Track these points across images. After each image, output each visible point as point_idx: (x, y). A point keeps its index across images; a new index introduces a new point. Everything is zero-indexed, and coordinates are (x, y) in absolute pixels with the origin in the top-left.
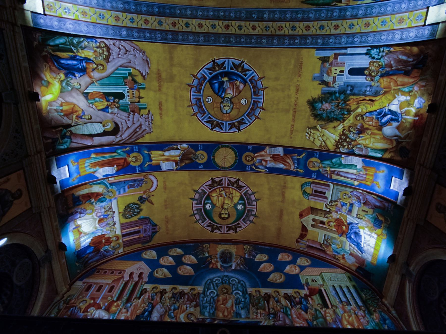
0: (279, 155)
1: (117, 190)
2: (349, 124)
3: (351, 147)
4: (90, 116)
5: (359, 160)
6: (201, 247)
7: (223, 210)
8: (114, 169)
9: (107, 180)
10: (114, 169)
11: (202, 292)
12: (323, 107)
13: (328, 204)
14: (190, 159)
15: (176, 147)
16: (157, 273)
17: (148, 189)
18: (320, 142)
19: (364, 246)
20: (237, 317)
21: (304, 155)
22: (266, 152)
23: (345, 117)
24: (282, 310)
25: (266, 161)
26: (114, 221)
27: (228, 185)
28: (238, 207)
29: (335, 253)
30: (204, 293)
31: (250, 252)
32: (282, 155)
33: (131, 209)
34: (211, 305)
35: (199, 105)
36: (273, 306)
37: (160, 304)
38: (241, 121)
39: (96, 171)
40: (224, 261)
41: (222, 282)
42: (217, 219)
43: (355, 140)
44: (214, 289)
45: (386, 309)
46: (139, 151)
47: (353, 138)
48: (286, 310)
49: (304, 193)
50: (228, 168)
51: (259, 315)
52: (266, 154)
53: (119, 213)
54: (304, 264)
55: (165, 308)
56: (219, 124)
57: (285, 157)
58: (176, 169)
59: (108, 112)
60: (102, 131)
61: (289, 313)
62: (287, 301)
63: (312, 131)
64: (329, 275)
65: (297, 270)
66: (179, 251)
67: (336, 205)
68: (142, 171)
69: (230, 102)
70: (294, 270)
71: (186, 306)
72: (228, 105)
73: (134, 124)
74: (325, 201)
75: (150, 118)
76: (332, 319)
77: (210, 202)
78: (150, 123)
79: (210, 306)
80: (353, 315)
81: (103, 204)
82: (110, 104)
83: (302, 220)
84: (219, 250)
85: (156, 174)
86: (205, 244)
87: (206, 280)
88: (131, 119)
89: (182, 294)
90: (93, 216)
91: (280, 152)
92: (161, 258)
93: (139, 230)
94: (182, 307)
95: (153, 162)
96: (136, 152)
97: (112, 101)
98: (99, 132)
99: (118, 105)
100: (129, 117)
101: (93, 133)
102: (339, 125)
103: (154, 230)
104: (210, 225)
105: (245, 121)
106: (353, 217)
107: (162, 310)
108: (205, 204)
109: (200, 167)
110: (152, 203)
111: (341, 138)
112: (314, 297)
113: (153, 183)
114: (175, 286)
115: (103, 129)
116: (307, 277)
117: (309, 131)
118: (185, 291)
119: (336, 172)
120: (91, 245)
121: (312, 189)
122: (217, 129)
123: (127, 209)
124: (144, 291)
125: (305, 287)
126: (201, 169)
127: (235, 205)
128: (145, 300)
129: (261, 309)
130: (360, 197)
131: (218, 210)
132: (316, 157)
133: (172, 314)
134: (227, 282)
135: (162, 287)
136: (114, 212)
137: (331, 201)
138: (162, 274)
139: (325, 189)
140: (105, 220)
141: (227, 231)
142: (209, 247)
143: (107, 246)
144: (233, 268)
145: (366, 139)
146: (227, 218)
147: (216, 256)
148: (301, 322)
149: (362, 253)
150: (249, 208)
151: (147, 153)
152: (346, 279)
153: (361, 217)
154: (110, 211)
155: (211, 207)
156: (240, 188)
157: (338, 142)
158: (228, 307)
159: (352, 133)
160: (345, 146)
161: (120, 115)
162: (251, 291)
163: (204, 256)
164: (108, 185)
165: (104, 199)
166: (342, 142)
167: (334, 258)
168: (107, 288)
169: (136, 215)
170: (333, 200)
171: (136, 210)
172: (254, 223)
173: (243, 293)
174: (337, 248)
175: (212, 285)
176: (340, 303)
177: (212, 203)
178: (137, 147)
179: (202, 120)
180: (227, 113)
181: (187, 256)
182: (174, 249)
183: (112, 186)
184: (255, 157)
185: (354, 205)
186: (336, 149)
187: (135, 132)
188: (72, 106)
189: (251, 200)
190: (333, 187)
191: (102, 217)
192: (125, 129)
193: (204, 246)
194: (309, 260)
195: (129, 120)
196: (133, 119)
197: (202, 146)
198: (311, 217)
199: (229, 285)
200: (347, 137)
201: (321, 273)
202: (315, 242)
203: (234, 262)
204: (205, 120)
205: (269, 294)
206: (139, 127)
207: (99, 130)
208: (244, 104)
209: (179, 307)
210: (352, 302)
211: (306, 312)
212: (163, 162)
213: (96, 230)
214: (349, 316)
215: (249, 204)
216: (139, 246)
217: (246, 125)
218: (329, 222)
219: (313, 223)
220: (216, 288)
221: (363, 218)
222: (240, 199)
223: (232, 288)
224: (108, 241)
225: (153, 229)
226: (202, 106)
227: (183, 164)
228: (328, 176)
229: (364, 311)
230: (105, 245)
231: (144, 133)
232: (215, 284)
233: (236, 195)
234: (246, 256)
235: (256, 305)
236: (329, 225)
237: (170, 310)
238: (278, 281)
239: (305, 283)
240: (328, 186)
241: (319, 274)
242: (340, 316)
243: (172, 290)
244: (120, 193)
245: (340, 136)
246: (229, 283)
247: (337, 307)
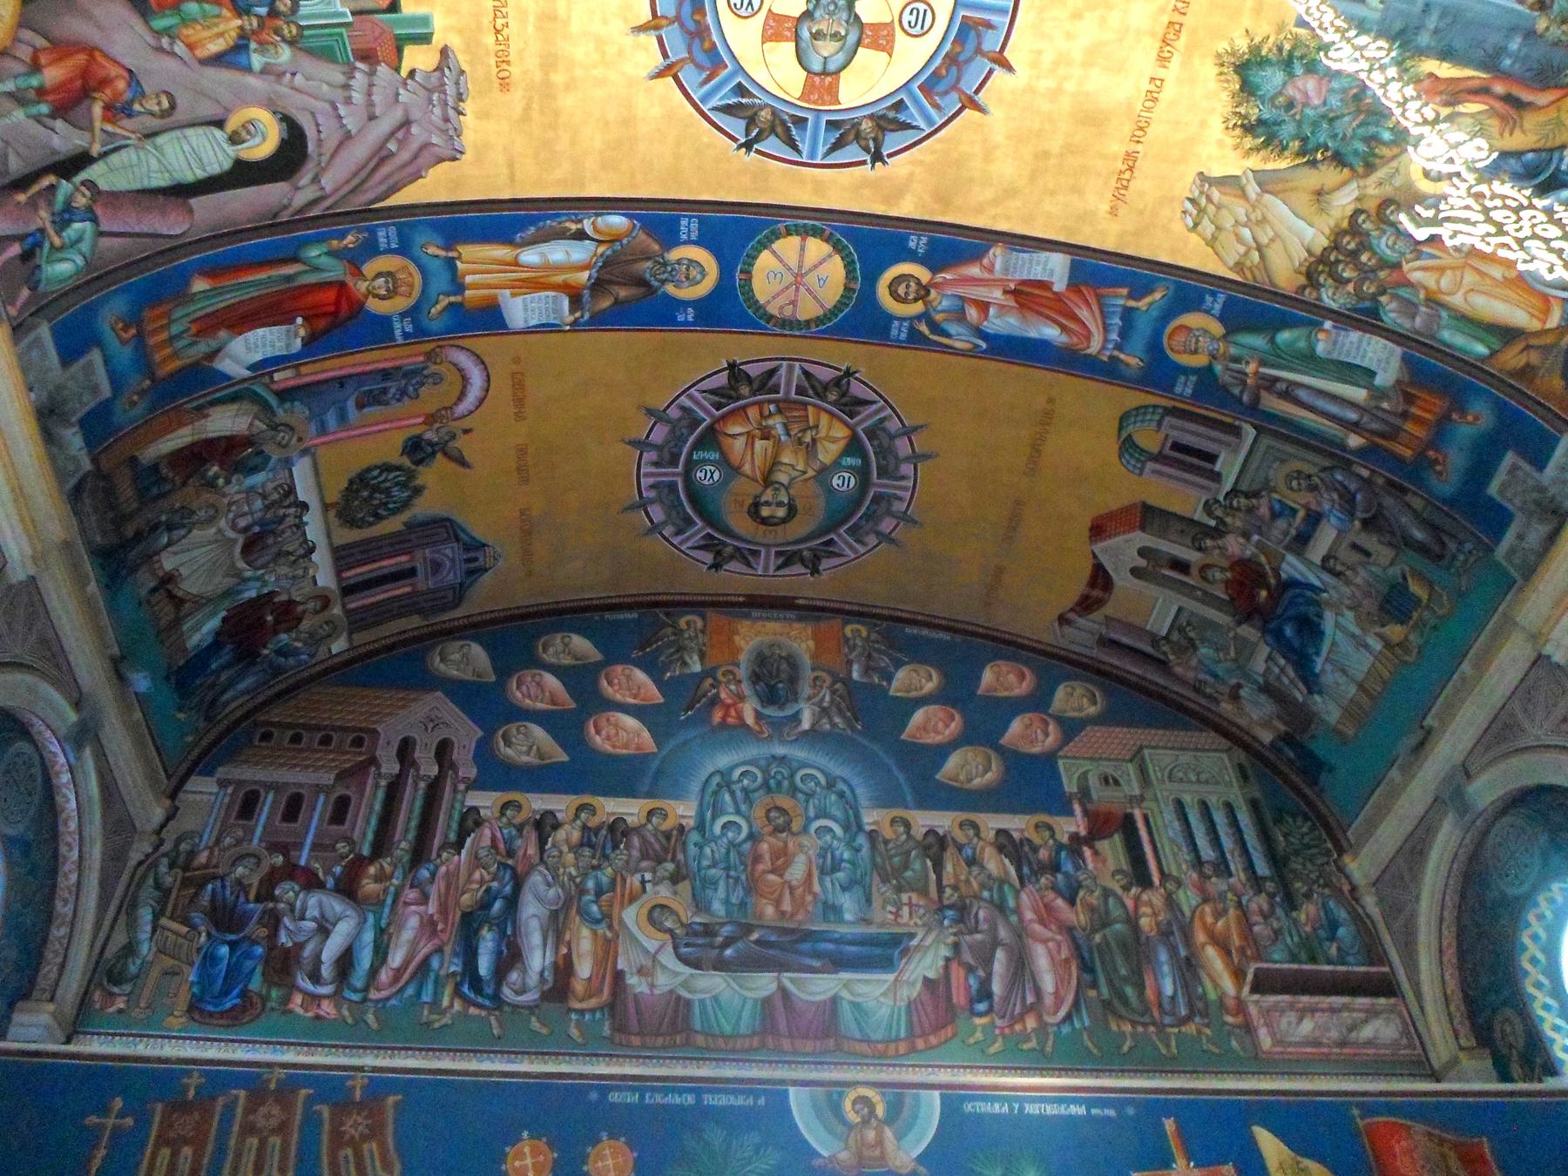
0: (1044, 285)
1: (310, 419)
2: (1387, 190)
3: (1372, 290)
4: (168, 94)
5: (1391, 353)
6: (669, 630)
7: (769, 492)
8: (296, 335)
9: (266, 380)
10: (296, 335)
11: (692, 823)
12: (1290, 91)
13: (1217, 501)
14: (641, 282)
15: (574, 227)
16: (508, 743)
17: (446, 408)
18: (1242, 249)
19: (1323, 670)
20: (826, 920)
21: (1158, 295)
22: (991, 270)
23: (1375, 155)
24: (986, 894)
25: (983, 306)
26: (306, 541)
27: (801, 391)
28: (836, 481)
29: (1202, 676)
30: (701, 826)
31: (869, 656)
32: (1060, 285)
33: (376, 489)
34: (732, 873)
35: (691, 26)
36: (956, 876)
37: (541, 868)
38: (891, 114)
39: (218, 351)
40: (770, 697)
41: (766, 785)
42: (740, 523)
43: (1397, 266)
44: (738, 812)
45: (1346, 888)
46: (404, 250)
47: (1388, 252)
48: (1003, 898)
49: (1128, 446)
50: (808, 322)
51: (906, 910)
52: (986, 275)
53: (326, 507)
54: (1081, 709)
55: (563, 886)
56: (783, 123)
57: (1072, 296)
58: (575, 323)
59: (248, 69)
60: (227, 165)
61: (1011, 903)
62: (1007, 861)
63: (1216, 194)
64: (1166, 758)
65: (1049, 739)
66: (580, 643)
67: (1250, 510)
68: (420, 333)
69: (844, 16)
70: (1040, 736)
71: (638, 877)
72: (835, 28)
73: (372, 117)
74: (1208, 489)
75: (450, 89)
76: (1158, 924)
77: (714, 456)
78: (451, 113)
79: (728, 876)
80: (1232, 912)
81: (258, 479)
82: (255, 22)
83: (1098, 548)
84: (742, 643)
85: (484, 344)
86: (688, 613)
87: (704, 775)
88: (357, 97)
89: (618, 830)
90: (220, 531)
91: (1052, 272)
92: (510, 675)
93: (408, 566)
94: (624, 880)
95: (468, 293)
96: (389, 251)
97: (263, 11)
98: (214, 169)
99: (294, 31)
100: (346, 87)
101: (189, 177)
102: (1344, 184)
103: (472, 565)
104: (708, 544)
105: (912, 116)
106: (1309, 563)
107: (552, 892)
108: (691, 466)
109: (680, 318)
110: (462, 462)
111: (1336, 246)
112: (1104, 845)
113: (465, 380)
114: (587, 799)
115: (232, 151)
116: (1087, 766)
117: (1202, 193)
118: (629, 820)
119: (1281, 386)
121: (1161, 436)
122: (772, 144)
123: (357, 491)
124: (470, 821)
125: (1077, 808)
126: (686, 323)
127: (824, 472)
128: (483, 853)
129: (913, 890)
130: (1354, 497)
131: (746, 489)
132: (1208, 312)
133: (595, 908)
134: (786, 783)
135: (538, 803)
136: (304, 506)
137: (1234, 492)
138: (530, 748)
139: (1220, 442)
140: (270, 541)
141: (779, 568)
142: (703, 632)
143: (283, 636)
144: (806, 725)
145: (1441, 270)
146: (784, 521)
147: (736, 670)
148: (1048, 934)
149: (1310, 692)
150: (878, 485)
151: (442, 253)
152: (1231, 775)
153: (1339, 568)
154: (286, 503)
155: (716, 476)
156: (852, 406)
157: (1322, 259)
158: (794, 883)
159: (1390, 230)
160: (1349, 281)
161: (307, 79)
162: (875, 823)
163: (687, 671)
164: (273, 401)
165: (258, 460)
166: (1338, 261)
167: (1197, 690)
168: (321, 808)
169: (394, 512)
170: (1244, 486)
171: (395, 492)
172: (892, 541)
173: (846, 828)
174: (1220, 661)
175: (727, 797)
176: (1193, 867)
177: (725, 463)
178: (392, 231)
179: (704, 99)
180: (825, 73)
181: (619, 668)
182: (558, 638)
183: (288, 405)
184: (936, 286)
185: (1324, 521)
186: (1304, 288)
187: (381, 156)
188: (81, 58)
189: (896, 457)
190: (1255, 440)
191: (257, 529)
192: (331, 145)
193: (682, 623)
194: (1099, 699)
195: (348, 101)
196: (369, 94)
197: (695, 225)
198: (1141, 539)
199: (793, 796)
200: (1365, 246)
201: (1141, 748)
202: (1140, 631)
203: (809, 698)
204: (716, 101)
205: (941, 832)
206: (400, 135)
207: (213, 159)
208: (917, 30)
209: (613, 882)
210: (1236, 864)
211: (1072, 902)
212: (514, 295)
213: (234, 581)
214: (1218, 915)
215: (883, 472)
216: (415, 621)
217: (912, 136)
218: (1204, 568)
219: (1142, 563)
220: (743, 807)
221: (1349, 573)
222: (846, 452)
223: (806, 808)
224: (288, 614)
225: (469, 561)
226: (708, 29)
227: (606, 303)
228: (1245, 398)
229: (1271, 896)
230: (276, 633)
231: (420, 161)
232: (738, 793)
233: (832, 435)
234: (855, 675)
235: (893, 875)
236: (1205, 579)
237: (582, 891)
238: (977, 782)
239: (1075, 790)
240: (1236, 431)
241: (1132, 753)
242: (1188, 913)
243: (577, 816)
244: (323, 430)
245: (1338, 234)
246: (794, 790)
247: (1179, 884)
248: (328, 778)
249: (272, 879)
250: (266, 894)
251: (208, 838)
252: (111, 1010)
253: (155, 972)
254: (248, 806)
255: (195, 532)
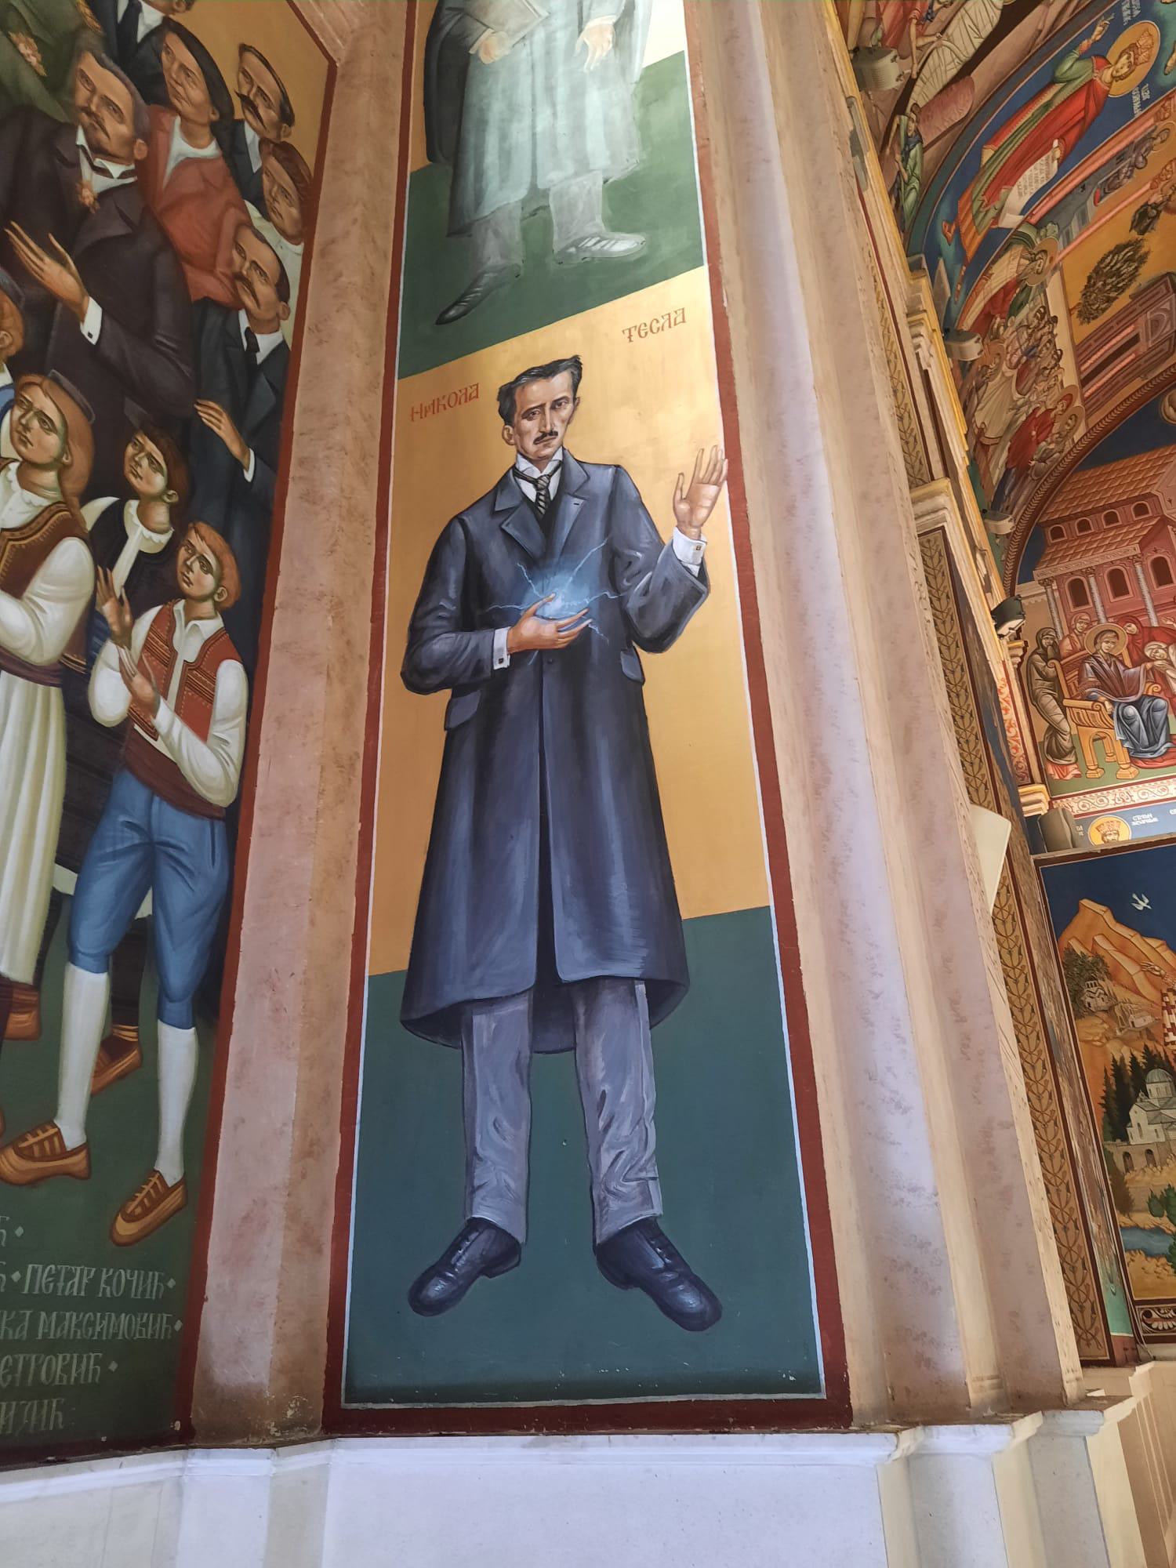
120: (1010, 466)
123: (1095, 284)
136: (1055, 320)
169: (1122, 290)
230: (1038, 443)
248: (1134, 549)
249: (1136, 646)
250: (1140, 659)
251: (1062, 628)
252: (1068, 778)
253: (1086, 743)
254: (1078, 593)
255: (990, 383)
